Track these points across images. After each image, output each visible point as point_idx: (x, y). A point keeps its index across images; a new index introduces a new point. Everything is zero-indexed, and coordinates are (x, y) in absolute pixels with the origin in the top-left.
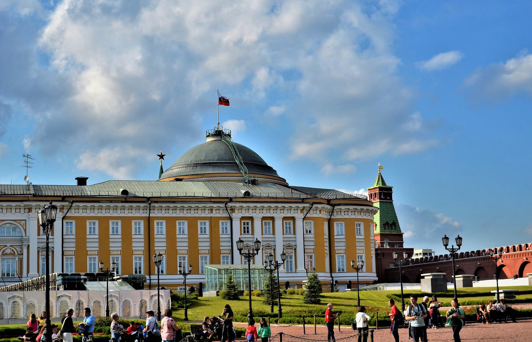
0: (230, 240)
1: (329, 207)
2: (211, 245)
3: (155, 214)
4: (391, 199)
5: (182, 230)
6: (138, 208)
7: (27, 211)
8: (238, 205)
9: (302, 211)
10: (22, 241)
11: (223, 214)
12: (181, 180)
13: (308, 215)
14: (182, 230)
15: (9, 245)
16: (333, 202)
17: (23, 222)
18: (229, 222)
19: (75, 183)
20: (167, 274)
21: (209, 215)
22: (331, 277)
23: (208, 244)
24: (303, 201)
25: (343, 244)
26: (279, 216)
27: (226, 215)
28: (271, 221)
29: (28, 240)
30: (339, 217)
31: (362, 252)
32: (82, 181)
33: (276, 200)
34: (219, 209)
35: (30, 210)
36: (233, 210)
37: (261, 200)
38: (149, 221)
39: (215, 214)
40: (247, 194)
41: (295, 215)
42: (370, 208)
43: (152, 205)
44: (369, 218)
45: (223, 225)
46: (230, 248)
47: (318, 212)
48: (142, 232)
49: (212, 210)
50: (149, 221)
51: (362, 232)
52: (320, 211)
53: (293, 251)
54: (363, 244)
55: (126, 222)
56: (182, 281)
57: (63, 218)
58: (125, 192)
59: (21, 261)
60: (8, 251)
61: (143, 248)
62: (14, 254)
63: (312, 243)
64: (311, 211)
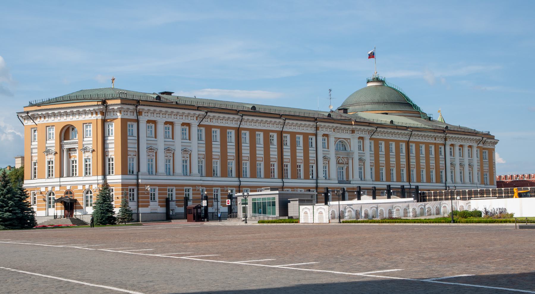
0: (136, 141)
7: (351, 132)
9: (476, 142)
10: (348, 154)
13: (202, 123)
17: (349, 140)
21: (435, 142)
22: (283, 182)
26: (178, 122)
28: (153, 125)
35: (353, 131)
42: (493, 141)
43: (287, 121)
44: (492, 147)
46: (136, 150)
47: (209, 120)
49: (435, 138)
52: (197, 117)
53: (189, 156)
56: (315, 185)
58: (392, 122)
60: (341, 161)
61: (276, 157)
64: (376, 134)
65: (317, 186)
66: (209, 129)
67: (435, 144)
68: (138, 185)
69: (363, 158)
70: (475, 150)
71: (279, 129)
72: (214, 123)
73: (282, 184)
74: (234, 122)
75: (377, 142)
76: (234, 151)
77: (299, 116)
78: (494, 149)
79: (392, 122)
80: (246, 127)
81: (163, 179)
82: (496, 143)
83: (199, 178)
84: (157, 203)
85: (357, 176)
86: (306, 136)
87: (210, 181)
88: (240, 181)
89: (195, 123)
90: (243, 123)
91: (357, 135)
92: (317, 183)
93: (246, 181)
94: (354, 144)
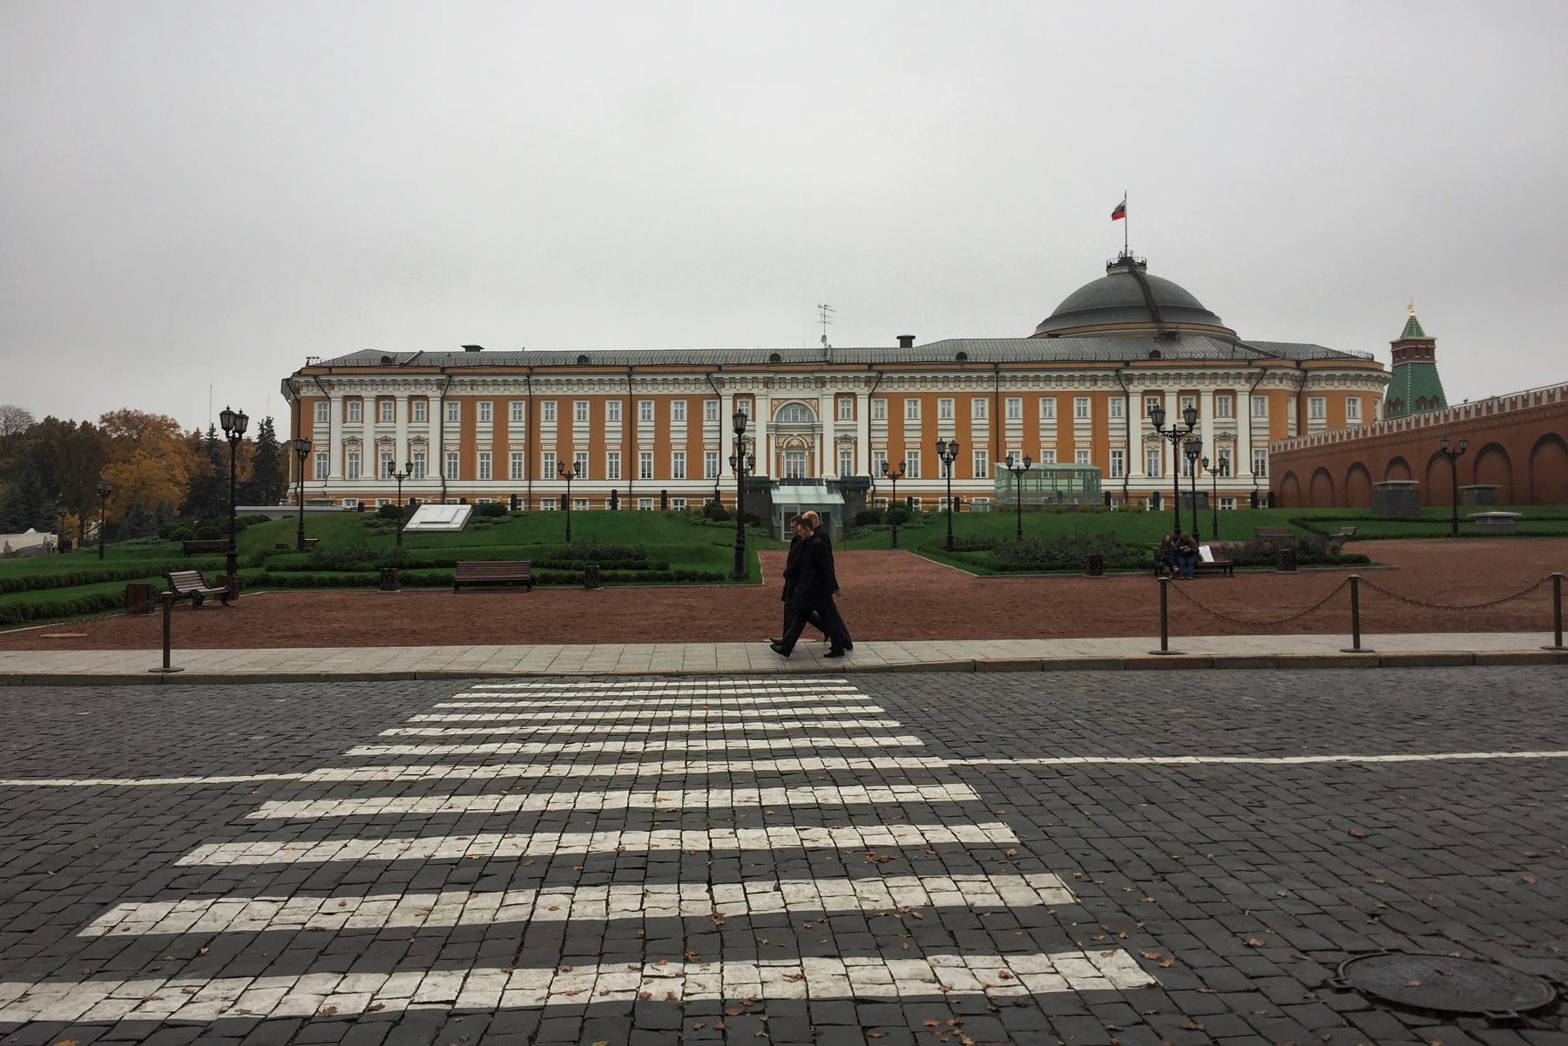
1: (1297, 373)
2: (1094, 436)
4: (1433, 358)
5: (1048, 414)
6: (980, 380)
8: (1137, 373)
12: (1056, 336)
14: (1048, 414)
16: (1304, 365)
19: (897, 344)
23: (1089, 433)
24: (1250, 363)
25: (1266, 432)
27: (1118, 388)
30: (1316, 388)
32: (906, 341)
33: (1204, 363)
34: (1106, 378)
36: (1130, 379)
37: (1178, 363)
38: (997, 401)
39: (1101, 387)
40: (1155, 355)
41: (1237, 387)
42: (1375, 374)
48: (987, 415)
50: (997, 401)
51: (1359, 413)
55: (963, 402)
57: (870, 396)
58: (962, 356)
59: (812, 456)
60: (795, 442)
62: (802, 448)
67: (1093, 394)
71: (625, 391)
72: (481, 391)
75: (896, 402)
76: (522, 436)
89: (434, 393)
91: (831, 390)
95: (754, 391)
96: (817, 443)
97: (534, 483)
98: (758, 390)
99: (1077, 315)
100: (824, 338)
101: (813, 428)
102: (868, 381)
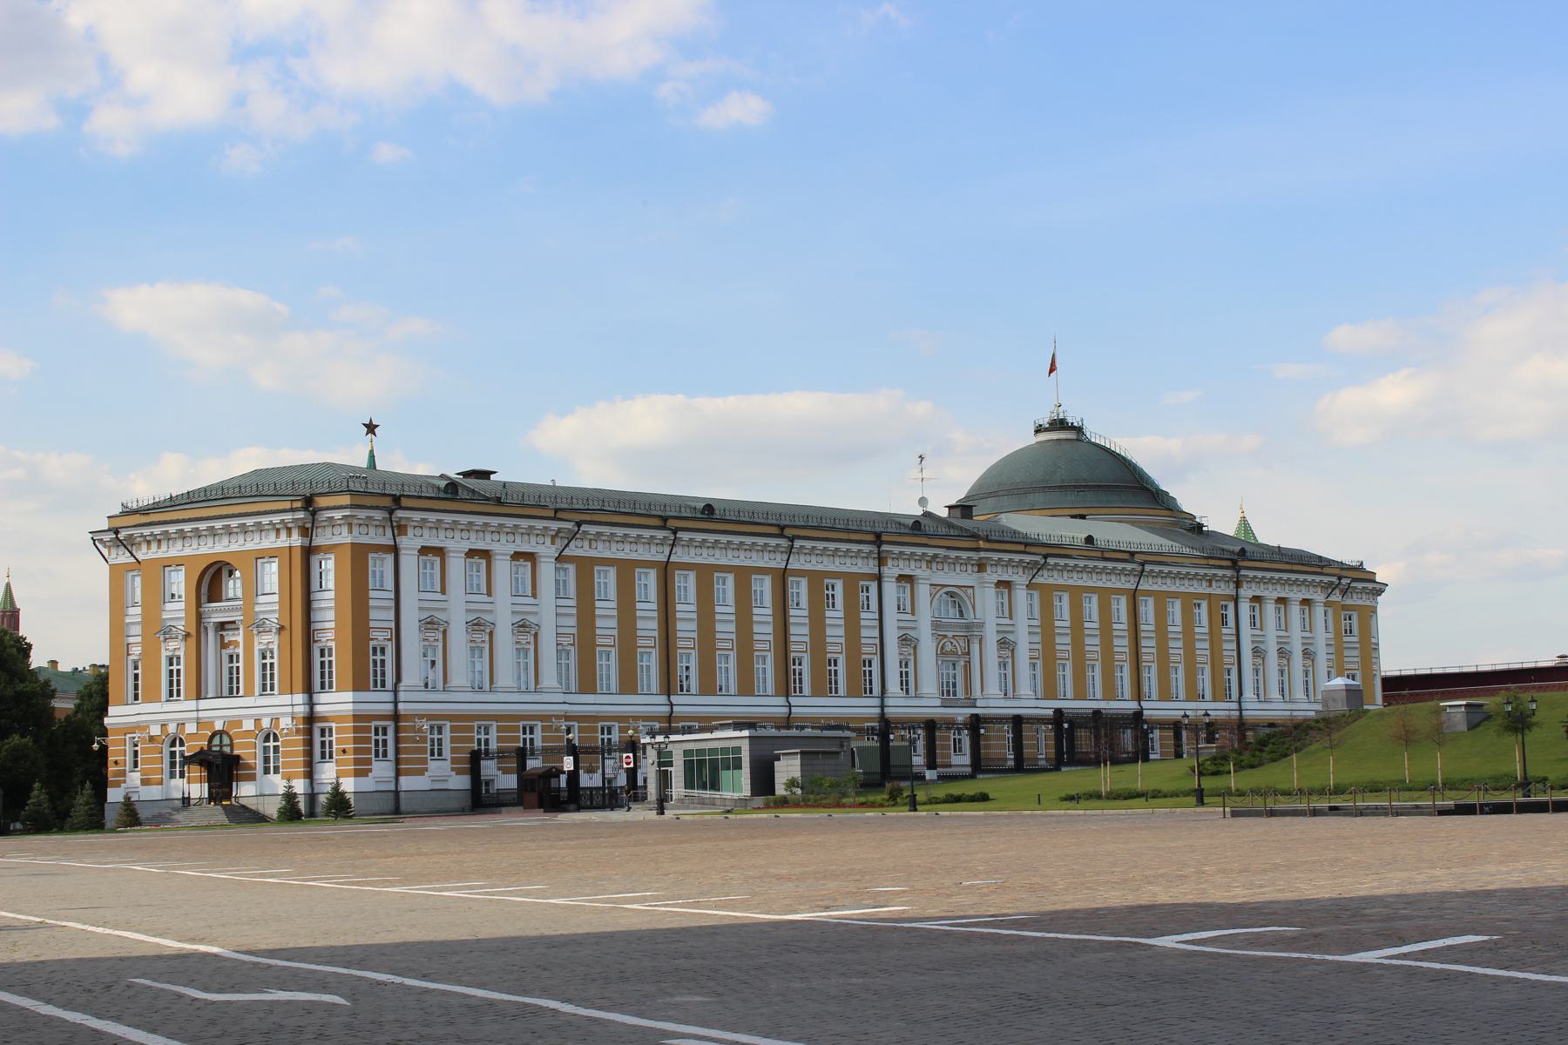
3: (1145, 585)
11: (870, 567)
15: (950, 634)
17: (970, 591)
18: (390, 558)
20: (849, 695)
21: (1208, 591)
22: (790, 706)
26: (503, 548)
29: (981, 625)
31: (838, 649)
35: (981, 567)
42: (1370, 586)
44: (1368, 603)
45: (381, 566)
47: (586, 544)
54: (1171, 644)
56: (878, 710)
58: (1090, 539)
60: (949, 647)
61: (771, 638)
63: (1356, 653)
65: (883, 714)
66: (586, 567)
68: (396, 717)
69: (912, 633)
70: (1319, 611)
71: (777, 562)
72: (602, 551)
73: (667, 709)
74: (533, 539)
76: (654, 625)
77: (833, 529)
78: (1374, 610)
79: (1090, 539)
80: (686, 559)
81: (462, 700)
82: (1380, 592)
83: (561, 698)
84: (448, 764)
85: (993, 688)
86: (851, 580)
87: (588, 704)
88: (672, 705)
89: (547, 551)
90: (678, 549)
91: (993, 576)
92: (882, 707)
93: (685, 704)
94: (986, 604)
95: (917, 572)
96: (975, 648)
97: (674, 699)
98: (920, 571)
99: (1011, 483)
100: (923, 501)
101: (968, 627)
102: (1027, 567)
